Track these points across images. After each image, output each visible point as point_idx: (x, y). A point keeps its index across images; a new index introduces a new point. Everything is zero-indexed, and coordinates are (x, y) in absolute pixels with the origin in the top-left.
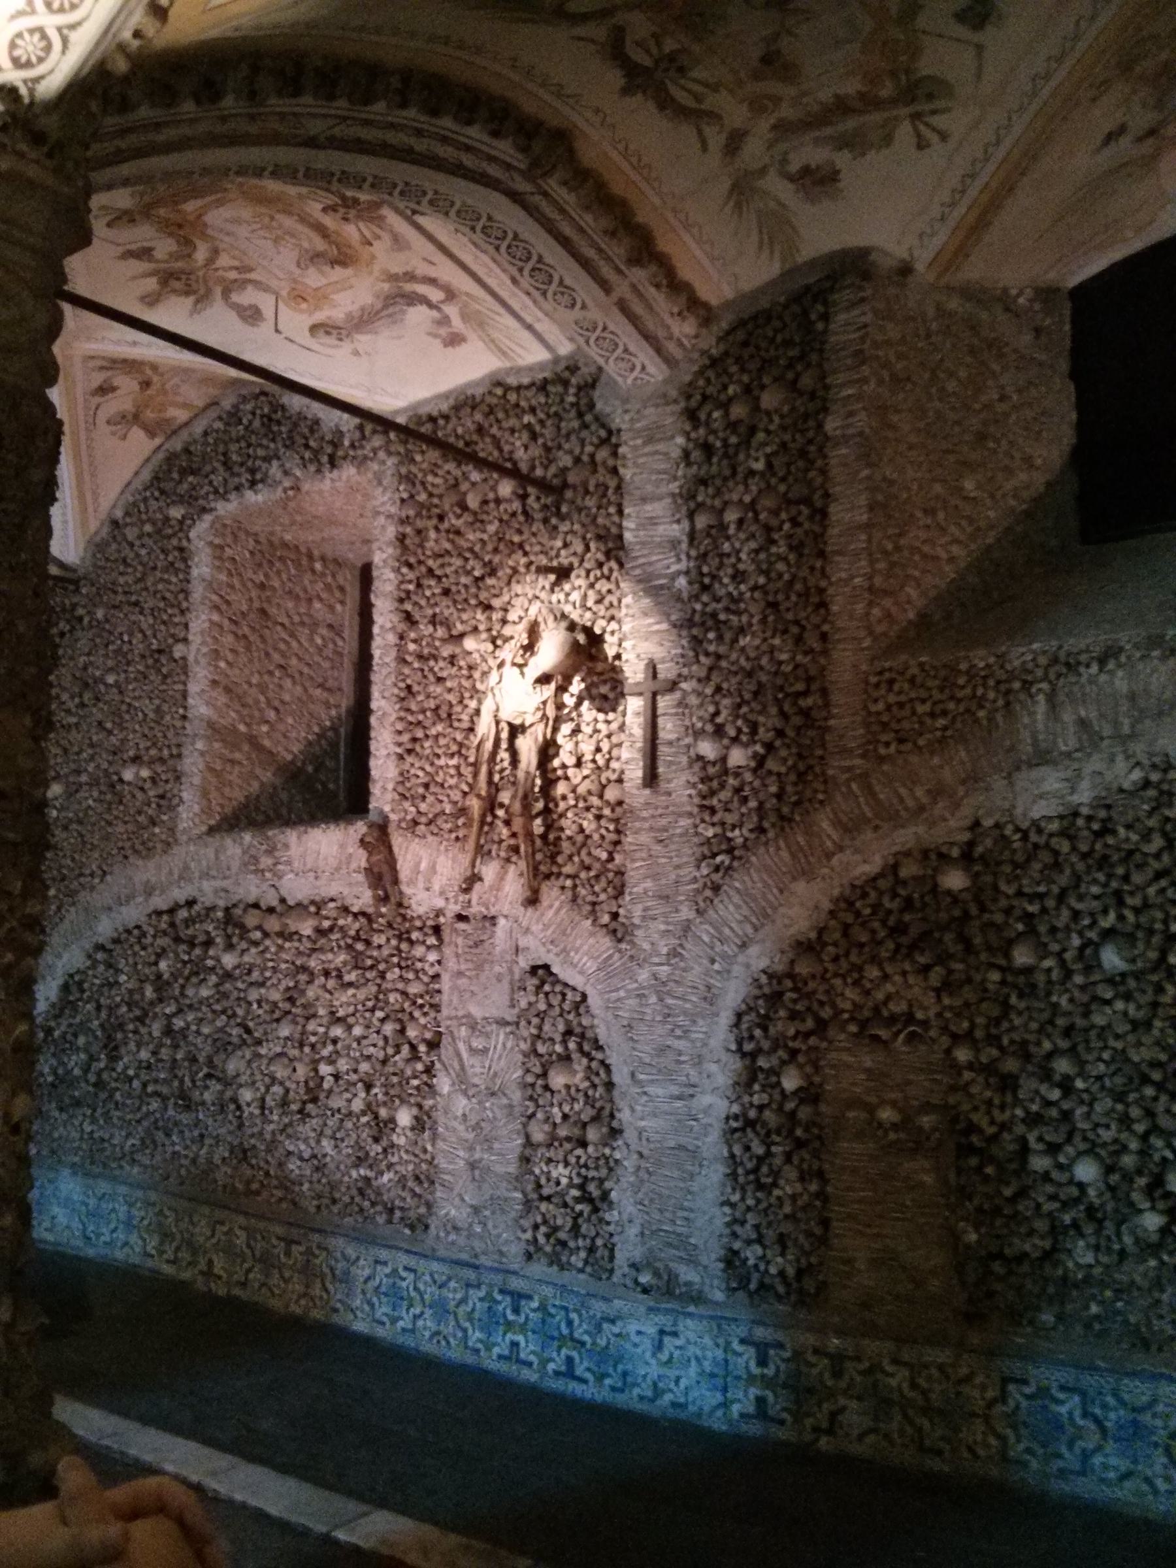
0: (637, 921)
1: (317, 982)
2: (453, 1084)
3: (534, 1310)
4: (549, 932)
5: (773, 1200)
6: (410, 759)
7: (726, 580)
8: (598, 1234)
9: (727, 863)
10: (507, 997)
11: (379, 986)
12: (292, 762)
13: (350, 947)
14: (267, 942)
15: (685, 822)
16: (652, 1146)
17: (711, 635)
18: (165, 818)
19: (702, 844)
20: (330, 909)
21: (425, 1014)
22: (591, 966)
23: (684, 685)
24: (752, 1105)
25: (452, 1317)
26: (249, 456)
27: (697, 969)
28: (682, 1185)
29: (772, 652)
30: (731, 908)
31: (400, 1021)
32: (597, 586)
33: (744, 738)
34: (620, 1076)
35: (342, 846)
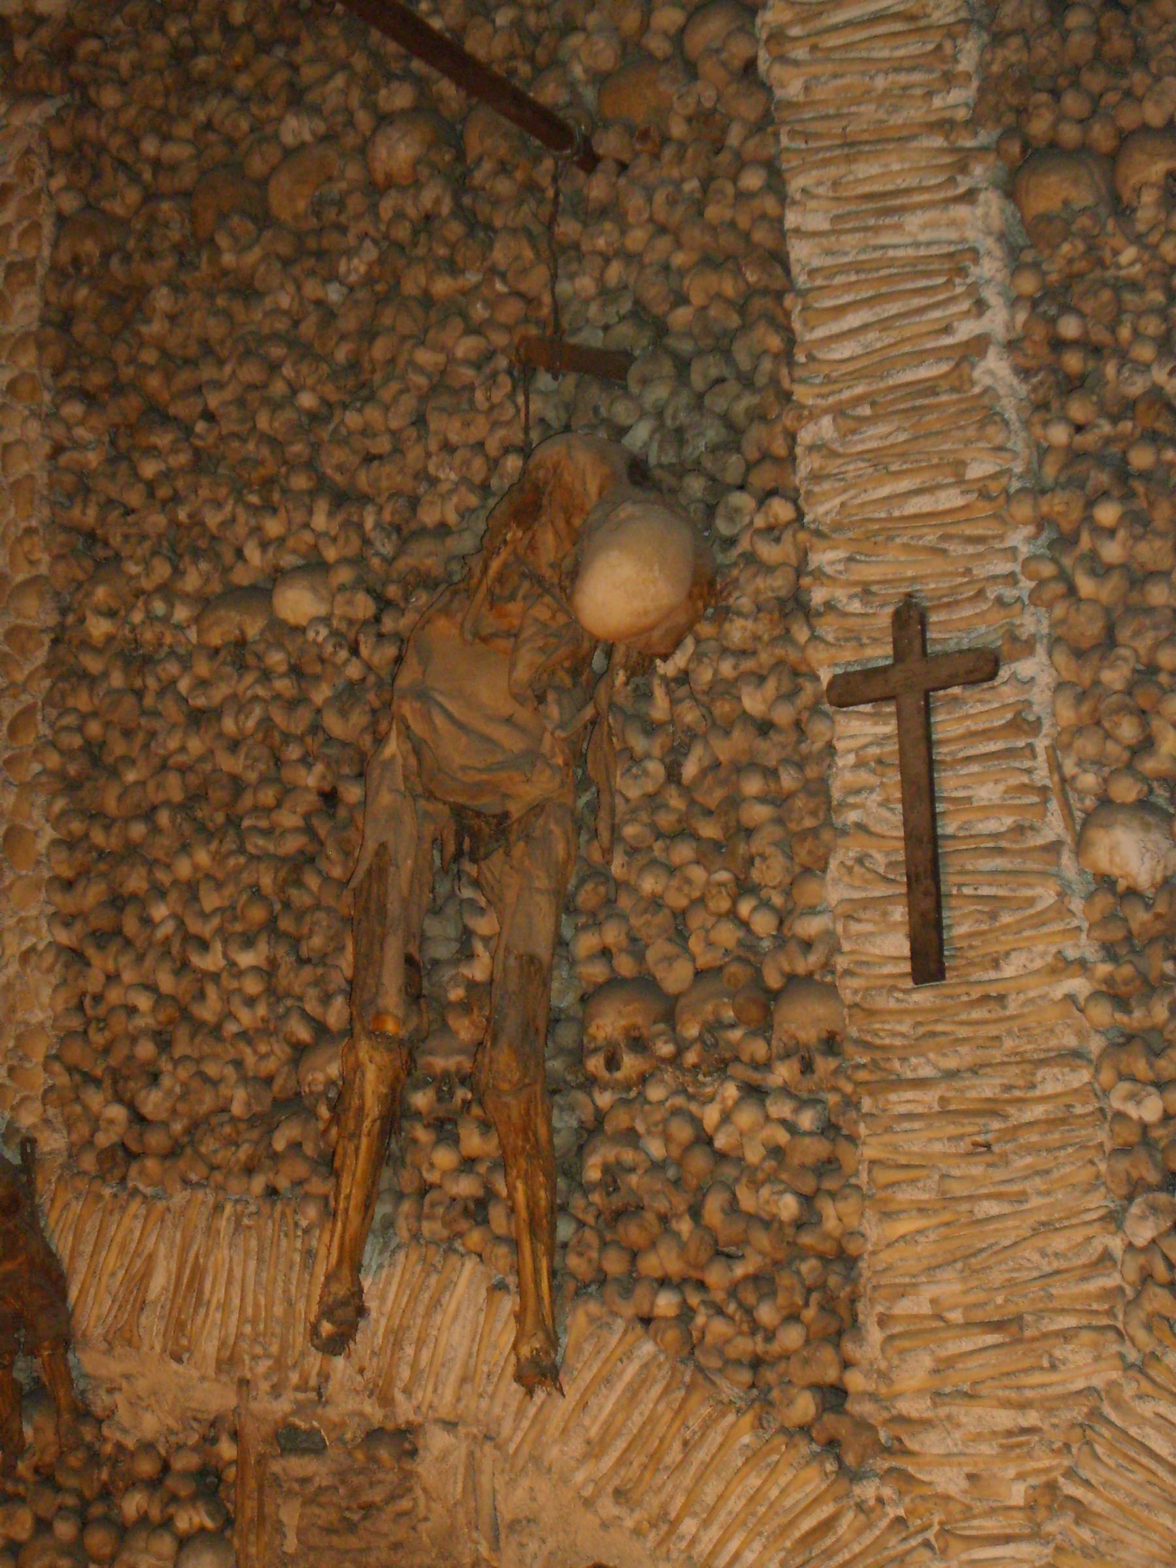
0: (908, 1407)
6: (101, 962)
15: (1052, 1082)
17: (1107, 514)
19: (1124, 1150)
23: (1026, 667)
32: (717, 402)
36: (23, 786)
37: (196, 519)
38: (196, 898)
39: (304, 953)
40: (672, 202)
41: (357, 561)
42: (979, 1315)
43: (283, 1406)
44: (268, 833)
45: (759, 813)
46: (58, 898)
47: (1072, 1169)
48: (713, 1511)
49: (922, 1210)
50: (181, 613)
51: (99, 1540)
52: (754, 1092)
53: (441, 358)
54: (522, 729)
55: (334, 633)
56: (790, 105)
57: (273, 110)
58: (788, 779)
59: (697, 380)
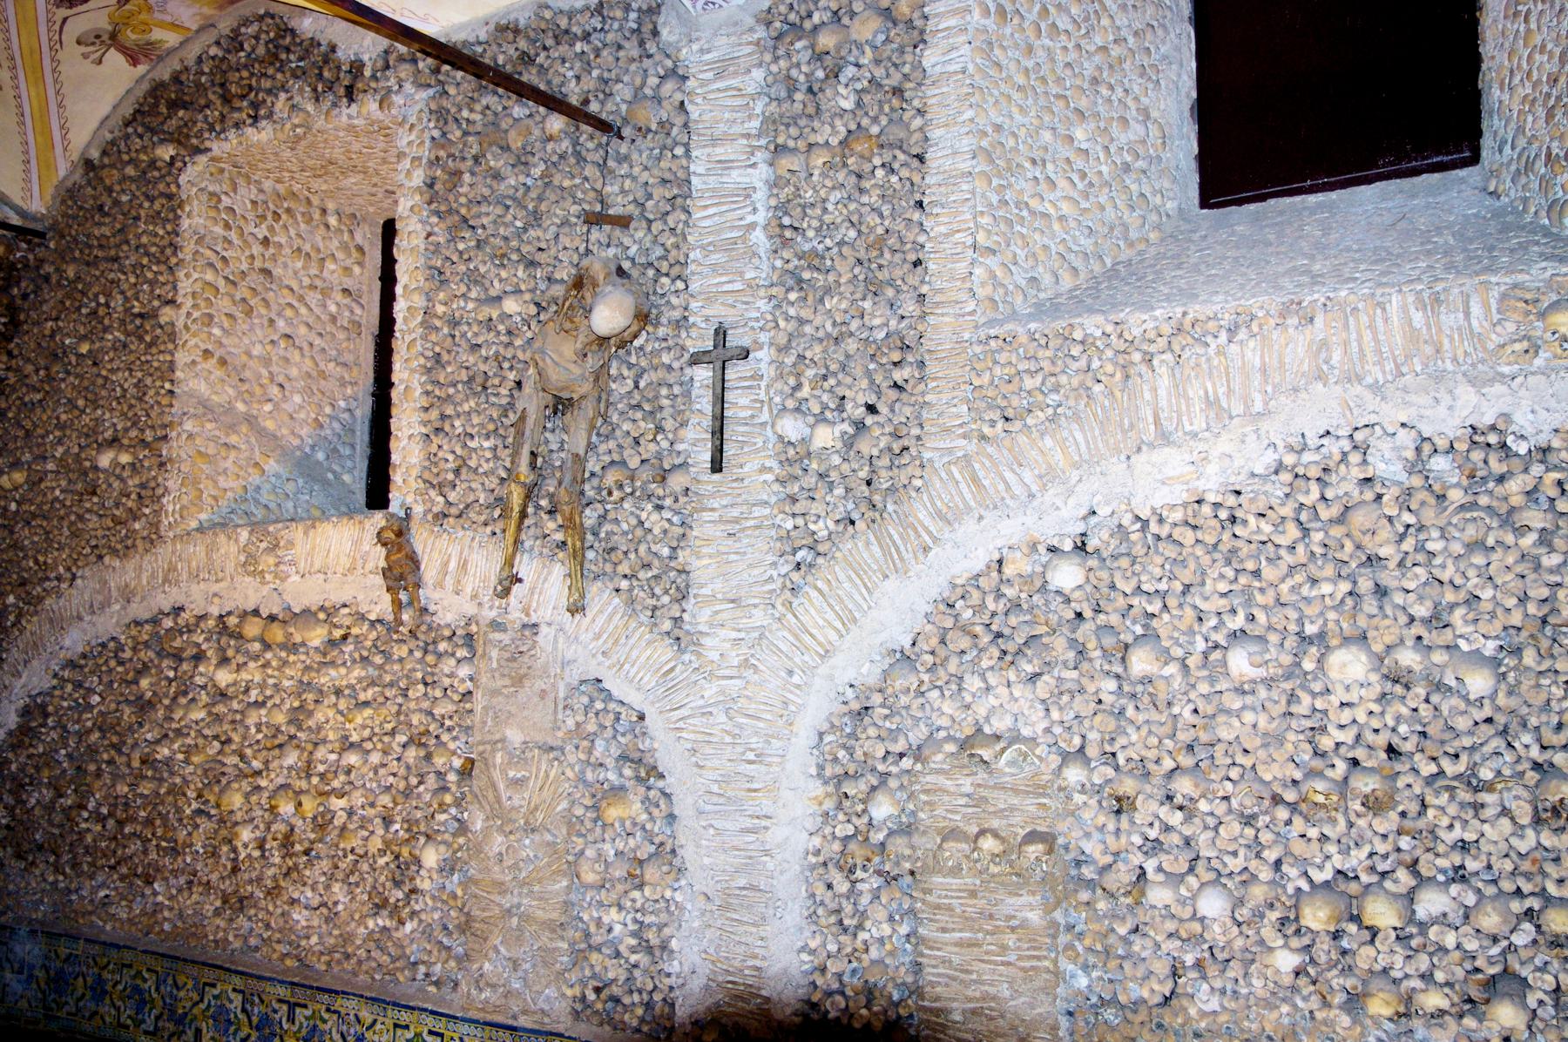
1: (326, 702)
4: (601, 641)
6: (436, 440)
7: (811, 234)
8: (655, 987)
10: (551, 717)
12: (299, 448)
14: (269, 655)
15: (758, 512)
17: (793, 296)
18: (147, 511)
19: (780, 539)
20: (343, 617)
21: (455, 739)
22: (650, 680)
24: (834, 837)
26: (251, 88)
28: (754, 930)
30: (812, 611)
31: (424, 745)
33: (828, 415)
34: (684, 806)
35: (357, 543)
37: (476, 269)
40: (649, 157)
43: (493, 614)
44: (497, 395)
45: (665, 402)
50: (471, 306)
51: (430, 659)
52: (659, 508)
56: (696, 122)
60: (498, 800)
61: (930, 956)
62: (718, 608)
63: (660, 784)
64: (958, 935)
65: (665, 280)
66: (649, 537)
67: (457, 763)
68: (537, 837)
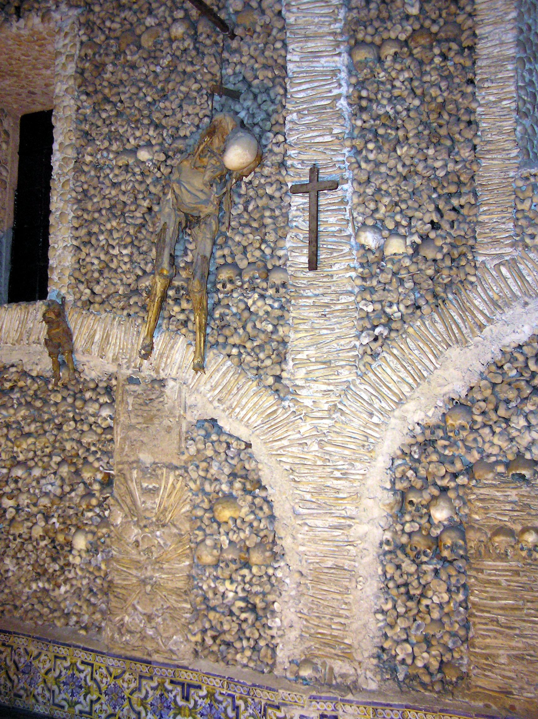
0: (298, 383)
2: (126, 516)
3: (203, 698)
4: (217, 392)
5: (422, 608)
6: (85, 250)
9: (386, 333)
10: (175, 446)
11: (56, 436)
13: (28, 404)
15: (344, 299)
16: (311, 567)
17: (371, 146)
19: (362, 318)
21: (98, 459)
22: (255, 420)
23: (345, 187)
24: (403, 531)
25: (126, 703)
27: (356, 423)
28: (339, 597)
29: (426, 160)
30: (388, 370)
31: (74, 464)
32: (264, 107)
35: (23, 322)
36: (65, 201)
37: (116, 130)
38: (111, 234)
39: (141, 250)
40: (255, 50)
41: (161, 144)
42: (320, 360)
43: (129, 372)
44: (132, 218)
45: (268, 221)
46: (74, 232)
47: (347, 323)
48: (244, 406)
49: (306, 331)
51: (78, 403)
52: (262, 297)
53: (187, 89)
54: (205, 193)
55: (154, 164)
57: (144, 15)
58: (277, 213)
59: (259, 100)
60: (134, 503)
61: (480, 617)
62: (312, 368)
63: (263, 494)
64: (504, 602)
65: (270, 135)
66: (254, 317)
67: (99, 476)
68: (166, 530)
